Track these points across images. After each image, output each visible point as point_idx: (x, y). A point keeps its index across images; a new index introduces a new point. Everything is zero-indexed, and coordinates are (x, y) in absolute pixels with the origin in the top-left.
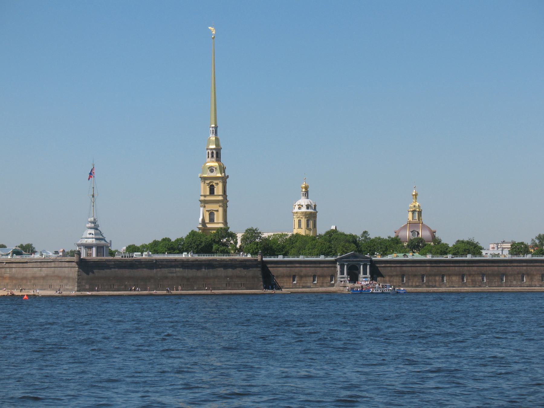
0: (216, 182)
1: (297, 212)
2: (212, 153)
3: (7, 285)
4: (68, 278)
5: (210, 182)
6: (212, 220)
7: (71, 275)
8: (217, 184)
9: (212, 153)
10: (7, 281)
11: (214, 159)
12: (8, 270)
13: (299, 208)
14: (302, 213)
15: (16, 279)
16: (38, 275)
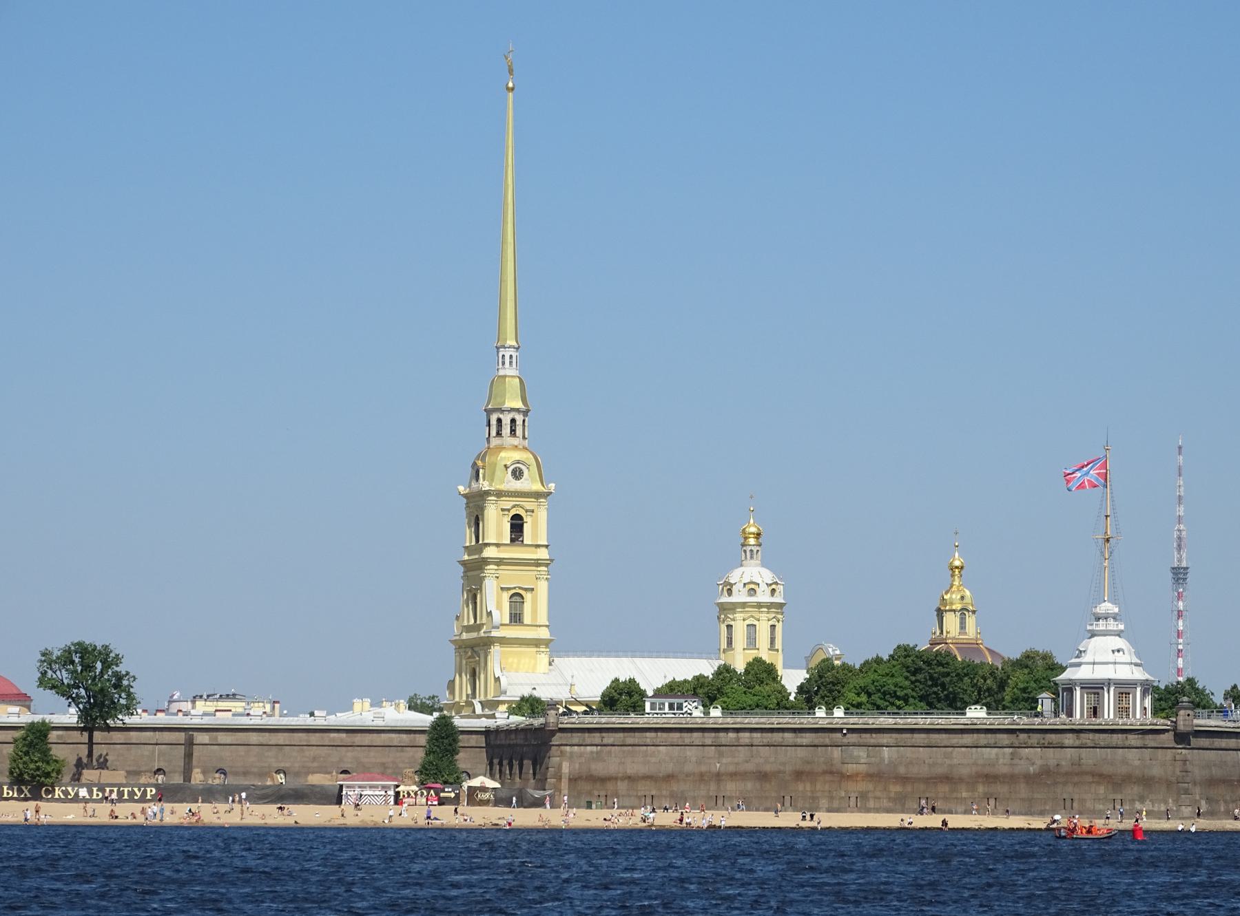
0: (529, 504)
1: (744, 605)
2: (513, 421)
3: (863, 796)
4: (1147, 782)
5: (514, 506)
6: (516, 618)
7: (1156, 771)
9: (513, 421)
10: (862, 786)
11: (515, 441)
12: (861, 753)
14: (759, 605)
15: (904, 780)
16: (1005, 770)
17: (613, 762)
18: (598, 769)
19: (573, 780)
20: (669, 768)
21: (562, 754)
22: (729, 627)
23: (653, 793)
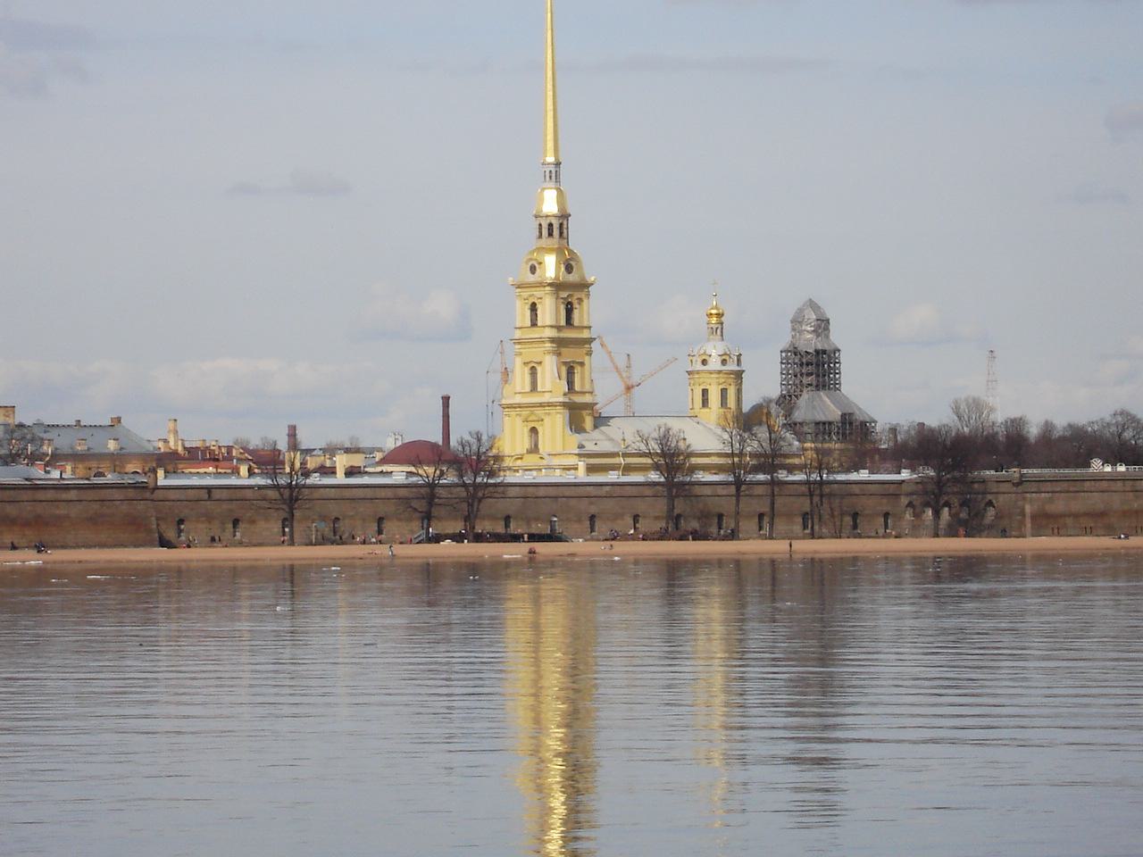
0: (577, 295)
8: (580, 300)
13: (724, 362)
17: (1059, 505)
18: (1051, 508)
19: (1034, 517)
20: (1100, 507)
21: (1024, 499)
22: (705, 392)
23: (1092, 525)
